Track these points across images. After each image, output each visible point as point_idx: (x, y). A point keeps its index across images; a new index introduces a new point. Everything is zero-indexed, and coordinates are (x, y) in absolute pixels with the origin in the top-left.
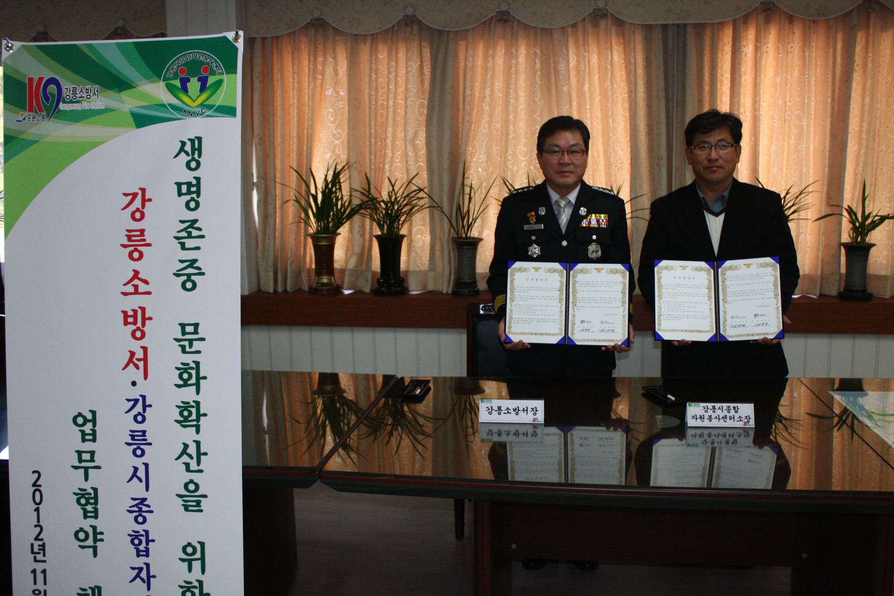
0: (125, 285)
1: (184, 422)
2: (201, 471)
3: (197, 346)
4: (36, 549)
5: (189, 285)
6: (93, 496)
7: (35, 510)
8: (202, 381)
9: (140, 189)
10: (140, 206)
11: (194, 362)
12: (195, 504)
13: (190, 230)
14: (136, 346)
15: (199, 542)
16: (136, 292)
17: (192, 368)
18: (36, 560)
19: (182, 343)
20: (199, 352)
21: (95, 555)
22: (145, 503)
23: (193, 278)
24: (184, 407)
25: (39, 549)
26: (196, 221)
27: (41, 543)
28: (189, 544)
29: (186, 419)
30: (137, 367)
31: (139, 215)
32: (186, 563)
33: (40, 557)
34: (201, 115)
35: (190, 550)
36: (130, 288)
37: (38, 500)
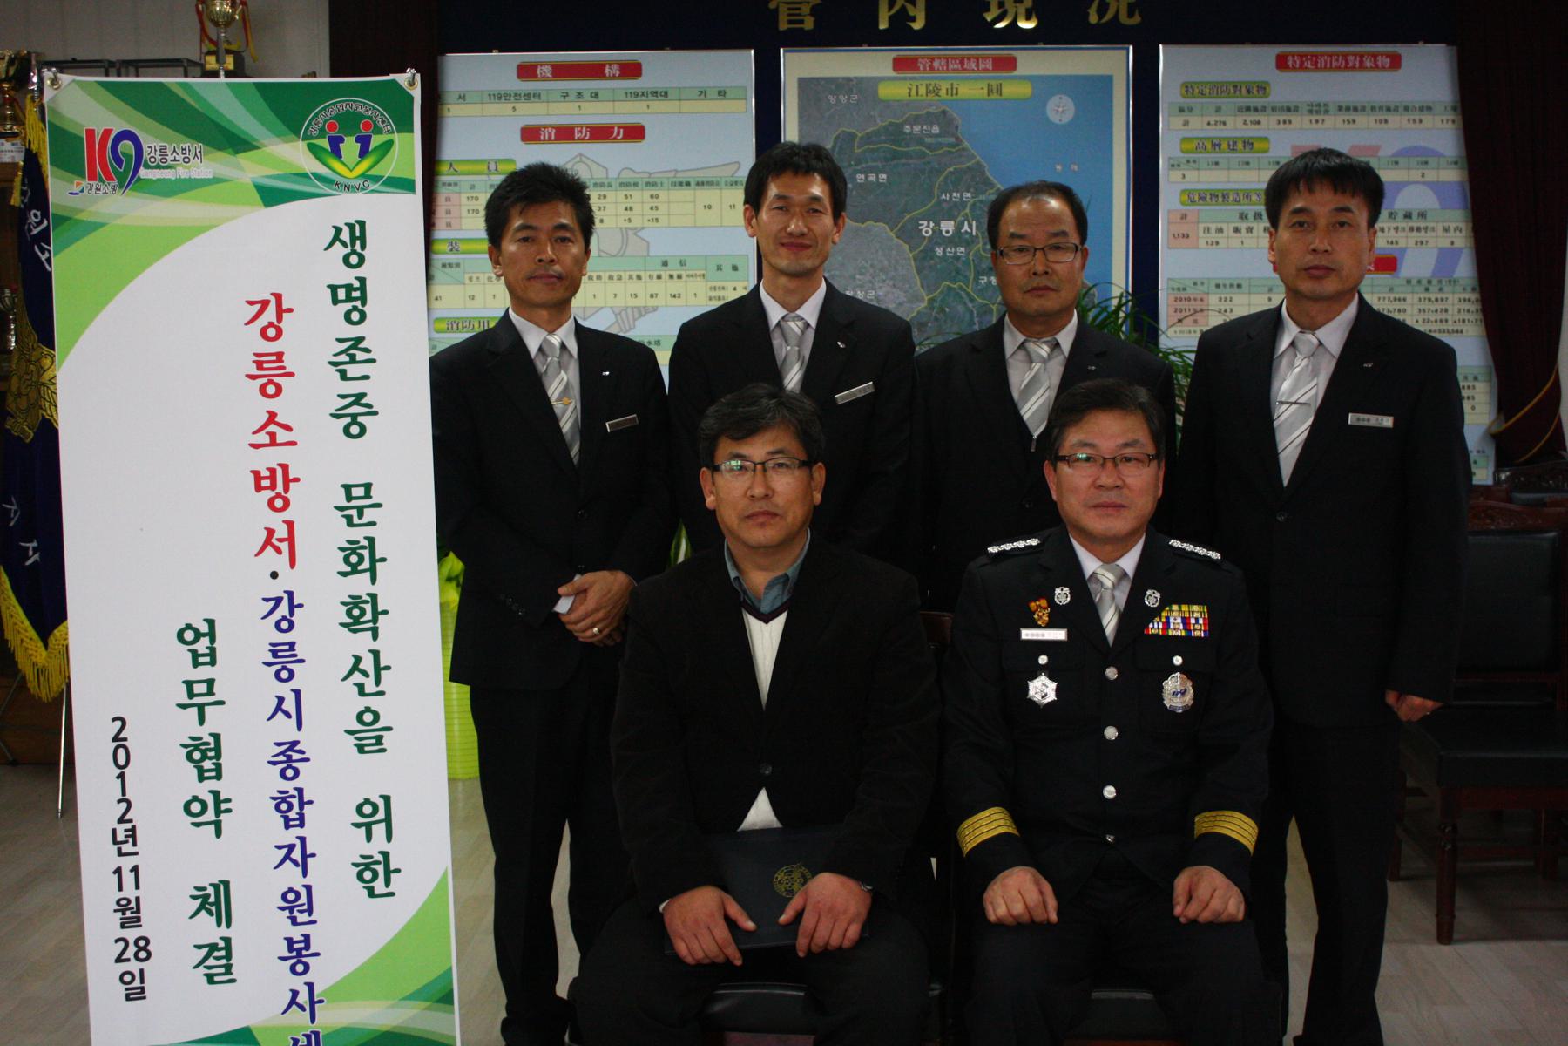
0: (254, 433)
1: (353, 625)
2: (382, 693)
3: (369, 515)
4: (120, 837)
5: (354, 428)
6: (212, 746)
7: (118, 777)
8: (379, 565)
9: (273, 294)
11: (366, 538)
12: (373, 741)
13: (353, 351)
14: (277, 522)
15: (381, 796)
16: (273, 441)
17: (364, 547)
18: (120, 853)
20: (373, 524)
21: (218, 834)
22: (297, 748)
23: (360, 419)
24: (354, 603)
26: (362, 339)
27: (128, 826)
28: (367, 801)
29: (357, 620)
30: (279, 551)
31: (273, 332)
32: (363, 829)
33: (127, 848)
34: (363, 189)
35: (367, 809)
36: (263, 438)
37: (122, 761)
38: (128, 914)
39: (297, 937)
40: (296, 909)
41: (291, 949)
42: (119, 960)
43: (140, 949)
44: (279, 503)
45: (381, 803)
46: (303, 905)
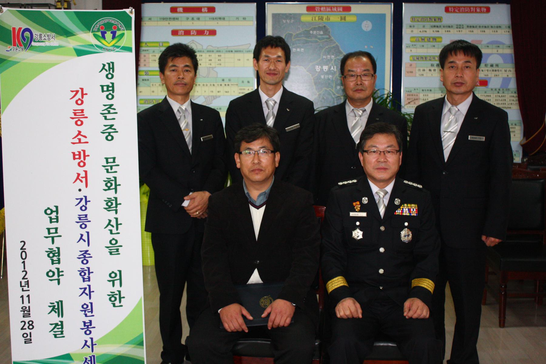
0: (73, 138)
2: (119, 233)
3: (115, 169)
4: (23, 284)
5: (109, 137)
6: (57, 252)
7: (22, 263)
8: (118, 187)
9: (80, 88)
10: (80, 97)
12: (115, 250)
13: (109, 109)
14: (81, 171)
15: (118, 270)
16: (80, 142)
17: (113, 180)
18: (23, 290)
19: (107, 168)
20: (116, 172)
21: (59, 283)
22: (88, 253)
23: (112, 134)
24: (109, 201)
25: (25, 284)
26: (112, 105)
27: (26, 280)
28: (113, 272)
29: (110, 207)
30: (82, 181)
31: (79, 102)
32: (111, 282)
33: (25, 288)
34: (113, 51)
35: (113, 275)
37: (24, 257)
38: (26, 312)
39: (87, 321)
40: (87, 311)
41: (85, 325)
42: (22, 329)
43: (30, 325)
44: (82, 164)
45: (118, 273)
46: (89, 309)
